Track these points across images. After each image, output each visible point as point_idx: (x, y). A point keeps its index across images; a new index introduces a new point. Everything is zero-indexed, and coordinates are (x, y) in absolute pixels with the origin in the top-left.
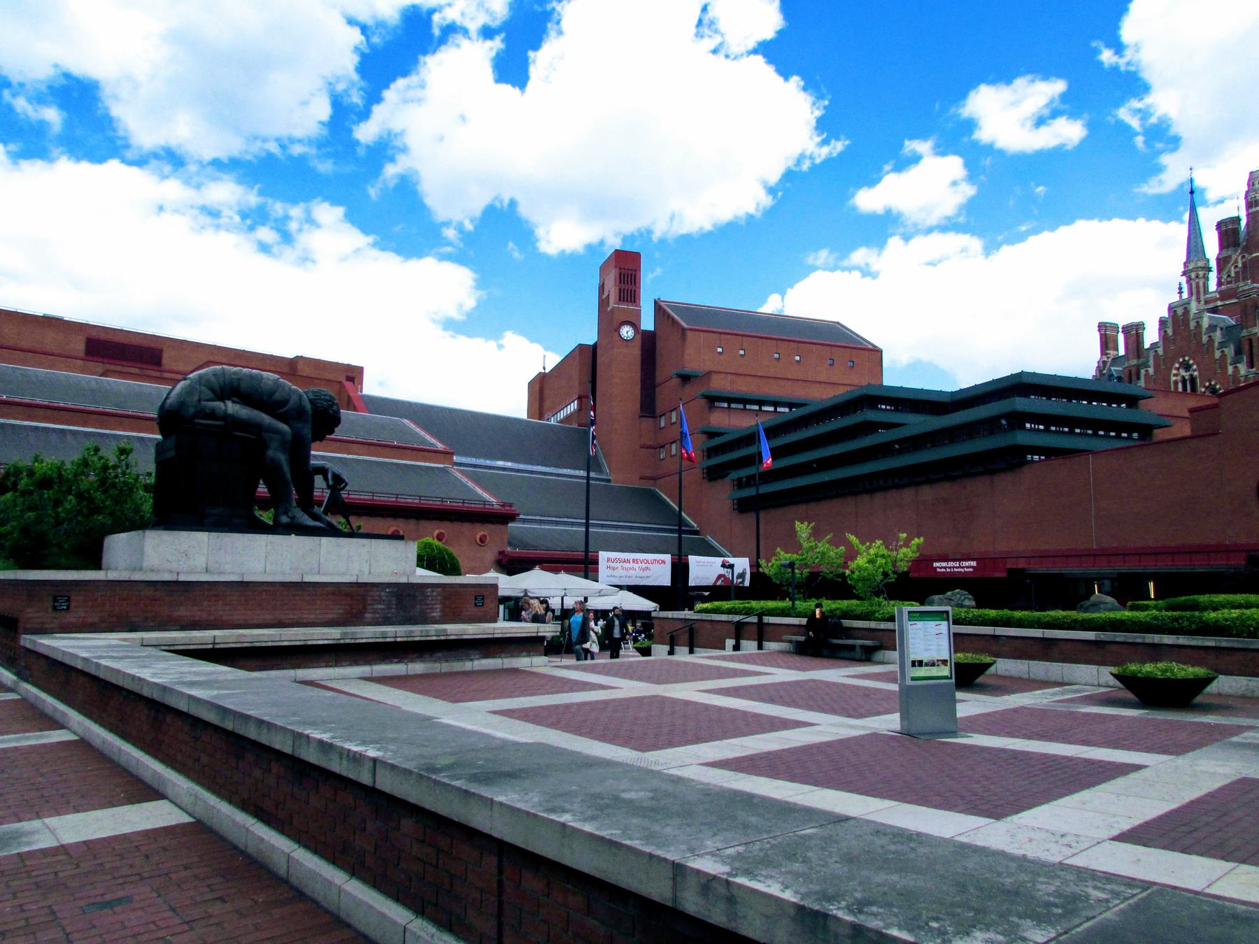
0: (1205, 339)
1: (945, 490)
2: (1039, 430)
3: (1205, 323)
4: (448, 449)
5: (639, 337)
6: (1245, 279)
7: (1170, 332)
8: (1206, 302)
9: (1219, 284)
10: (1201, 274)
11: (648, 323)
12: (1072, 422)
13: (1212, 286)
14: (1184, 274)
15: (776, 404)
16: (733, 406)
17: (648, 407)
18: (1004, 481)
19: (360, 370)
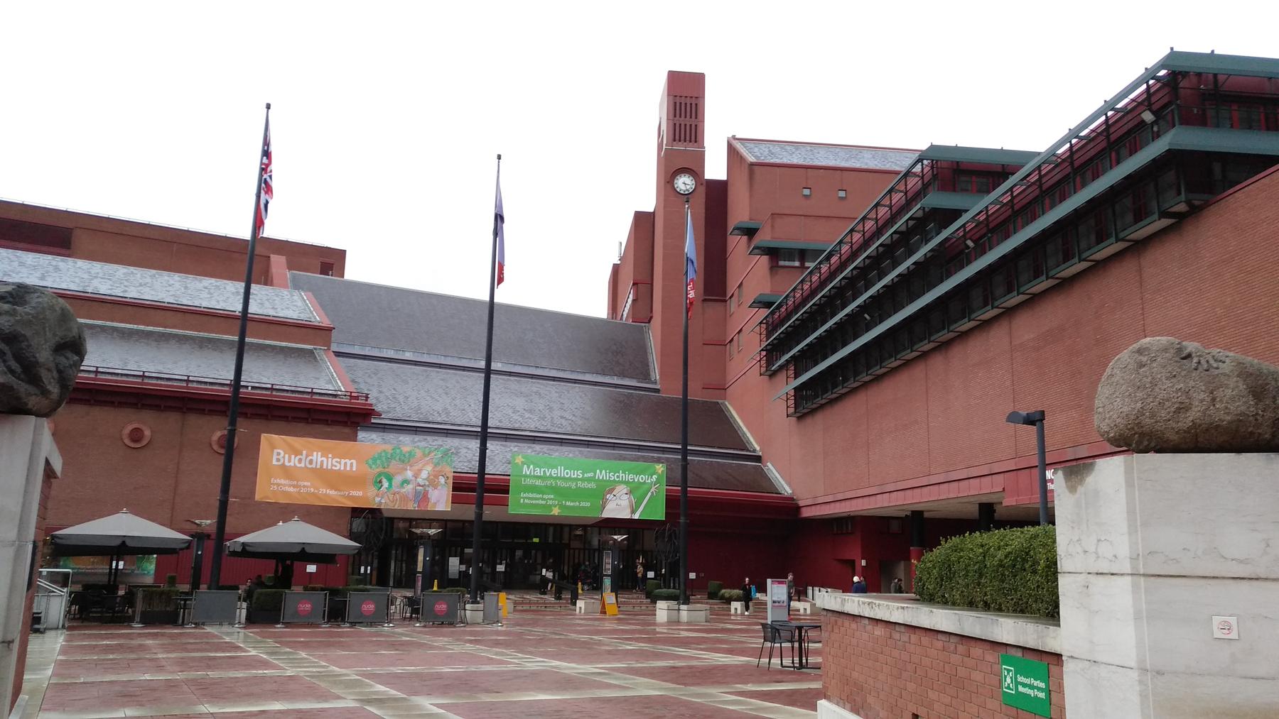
4: (326, 322)
5: (702, 190)
19: (342, 254)
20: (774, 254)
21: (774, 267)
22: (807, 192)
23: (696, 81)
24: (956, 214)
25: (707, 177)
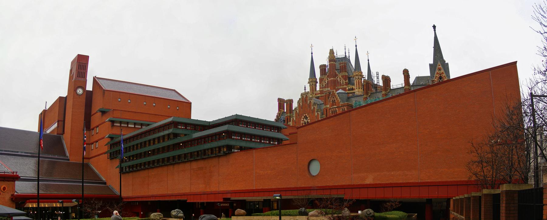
0: (312, 108)
1: (201, 164)
2: (257, 142)
3: (312, 101)
5: (85, 93)
6: (328, 87)
7: (301, 104)
8: (316, 94)
9: (320, 88)
10: (314, 84)
12: (251, 136)
13: (318, 88)
14: (309, 83)
15: (142, 125)
16: (122, 125)
17: (88, 125)
18: (223, 160)
20: (113, 122)
21: (113, 126)
22: (119, 100)
25: (87, 89)
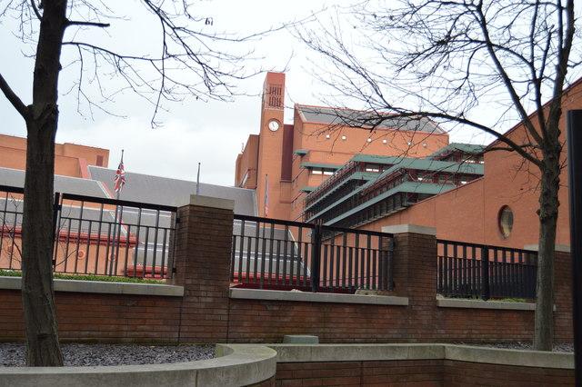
11: (288, 119)
17: (287, 175)
19: (107, 152)
20: (310, 169)
23: (281, 76)
24: (365, 182)
